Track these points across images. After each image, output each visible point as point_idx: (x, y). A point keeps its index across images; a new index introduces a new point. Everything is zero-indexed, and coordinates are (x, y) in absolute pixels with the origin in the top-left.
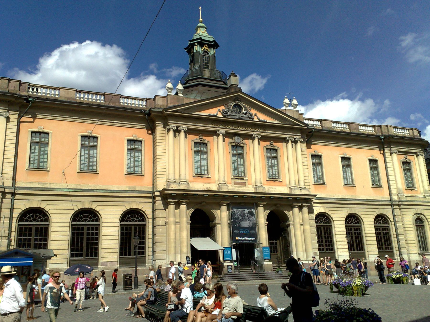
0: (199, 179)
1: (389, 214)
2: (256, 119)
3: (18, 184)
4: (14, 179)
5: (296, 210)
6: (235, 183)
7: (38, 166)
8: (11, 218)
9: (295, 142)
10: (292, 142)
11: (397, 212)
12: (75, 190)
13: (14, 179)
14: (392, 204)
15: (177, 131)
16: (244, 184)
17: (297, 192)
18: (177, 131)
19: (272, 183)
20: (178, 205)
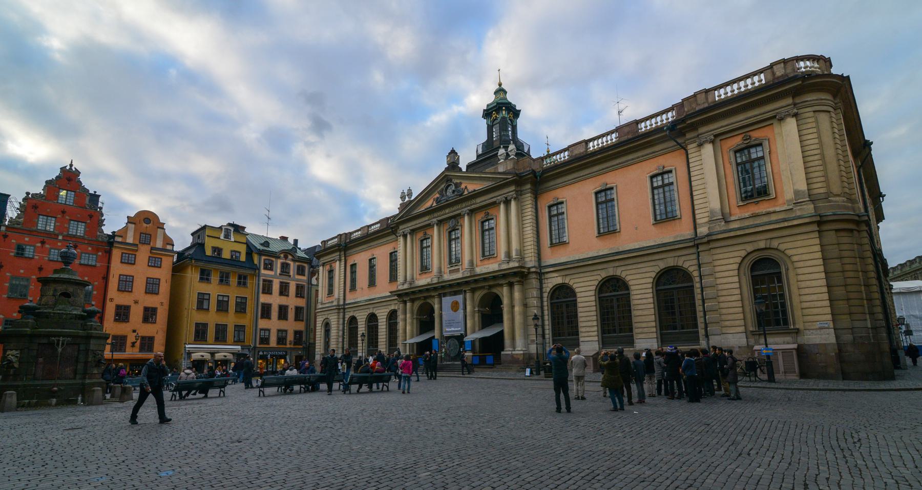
0: (425, 276)
1: (688, 263)
2: (466, 192)
3: (347, 302)
4: (344, 299)
5: (505, 290)
6: (451, 272)
7: (353, 288)
8: (344, 324)
9: (507, 202)
10: (504, 202)
11: (705, 258)
12: (366, 301)
13: (344, 299)
14: (697, 244)
15: (405, 236)
16: (458, 270)
17: (505, 266)
18: (405, 236)
19: (486, 262)
20: (405, 303)
